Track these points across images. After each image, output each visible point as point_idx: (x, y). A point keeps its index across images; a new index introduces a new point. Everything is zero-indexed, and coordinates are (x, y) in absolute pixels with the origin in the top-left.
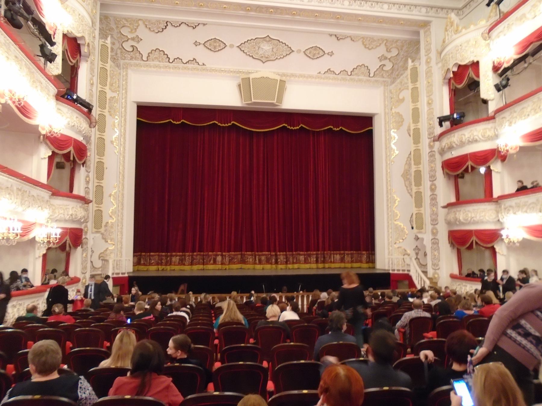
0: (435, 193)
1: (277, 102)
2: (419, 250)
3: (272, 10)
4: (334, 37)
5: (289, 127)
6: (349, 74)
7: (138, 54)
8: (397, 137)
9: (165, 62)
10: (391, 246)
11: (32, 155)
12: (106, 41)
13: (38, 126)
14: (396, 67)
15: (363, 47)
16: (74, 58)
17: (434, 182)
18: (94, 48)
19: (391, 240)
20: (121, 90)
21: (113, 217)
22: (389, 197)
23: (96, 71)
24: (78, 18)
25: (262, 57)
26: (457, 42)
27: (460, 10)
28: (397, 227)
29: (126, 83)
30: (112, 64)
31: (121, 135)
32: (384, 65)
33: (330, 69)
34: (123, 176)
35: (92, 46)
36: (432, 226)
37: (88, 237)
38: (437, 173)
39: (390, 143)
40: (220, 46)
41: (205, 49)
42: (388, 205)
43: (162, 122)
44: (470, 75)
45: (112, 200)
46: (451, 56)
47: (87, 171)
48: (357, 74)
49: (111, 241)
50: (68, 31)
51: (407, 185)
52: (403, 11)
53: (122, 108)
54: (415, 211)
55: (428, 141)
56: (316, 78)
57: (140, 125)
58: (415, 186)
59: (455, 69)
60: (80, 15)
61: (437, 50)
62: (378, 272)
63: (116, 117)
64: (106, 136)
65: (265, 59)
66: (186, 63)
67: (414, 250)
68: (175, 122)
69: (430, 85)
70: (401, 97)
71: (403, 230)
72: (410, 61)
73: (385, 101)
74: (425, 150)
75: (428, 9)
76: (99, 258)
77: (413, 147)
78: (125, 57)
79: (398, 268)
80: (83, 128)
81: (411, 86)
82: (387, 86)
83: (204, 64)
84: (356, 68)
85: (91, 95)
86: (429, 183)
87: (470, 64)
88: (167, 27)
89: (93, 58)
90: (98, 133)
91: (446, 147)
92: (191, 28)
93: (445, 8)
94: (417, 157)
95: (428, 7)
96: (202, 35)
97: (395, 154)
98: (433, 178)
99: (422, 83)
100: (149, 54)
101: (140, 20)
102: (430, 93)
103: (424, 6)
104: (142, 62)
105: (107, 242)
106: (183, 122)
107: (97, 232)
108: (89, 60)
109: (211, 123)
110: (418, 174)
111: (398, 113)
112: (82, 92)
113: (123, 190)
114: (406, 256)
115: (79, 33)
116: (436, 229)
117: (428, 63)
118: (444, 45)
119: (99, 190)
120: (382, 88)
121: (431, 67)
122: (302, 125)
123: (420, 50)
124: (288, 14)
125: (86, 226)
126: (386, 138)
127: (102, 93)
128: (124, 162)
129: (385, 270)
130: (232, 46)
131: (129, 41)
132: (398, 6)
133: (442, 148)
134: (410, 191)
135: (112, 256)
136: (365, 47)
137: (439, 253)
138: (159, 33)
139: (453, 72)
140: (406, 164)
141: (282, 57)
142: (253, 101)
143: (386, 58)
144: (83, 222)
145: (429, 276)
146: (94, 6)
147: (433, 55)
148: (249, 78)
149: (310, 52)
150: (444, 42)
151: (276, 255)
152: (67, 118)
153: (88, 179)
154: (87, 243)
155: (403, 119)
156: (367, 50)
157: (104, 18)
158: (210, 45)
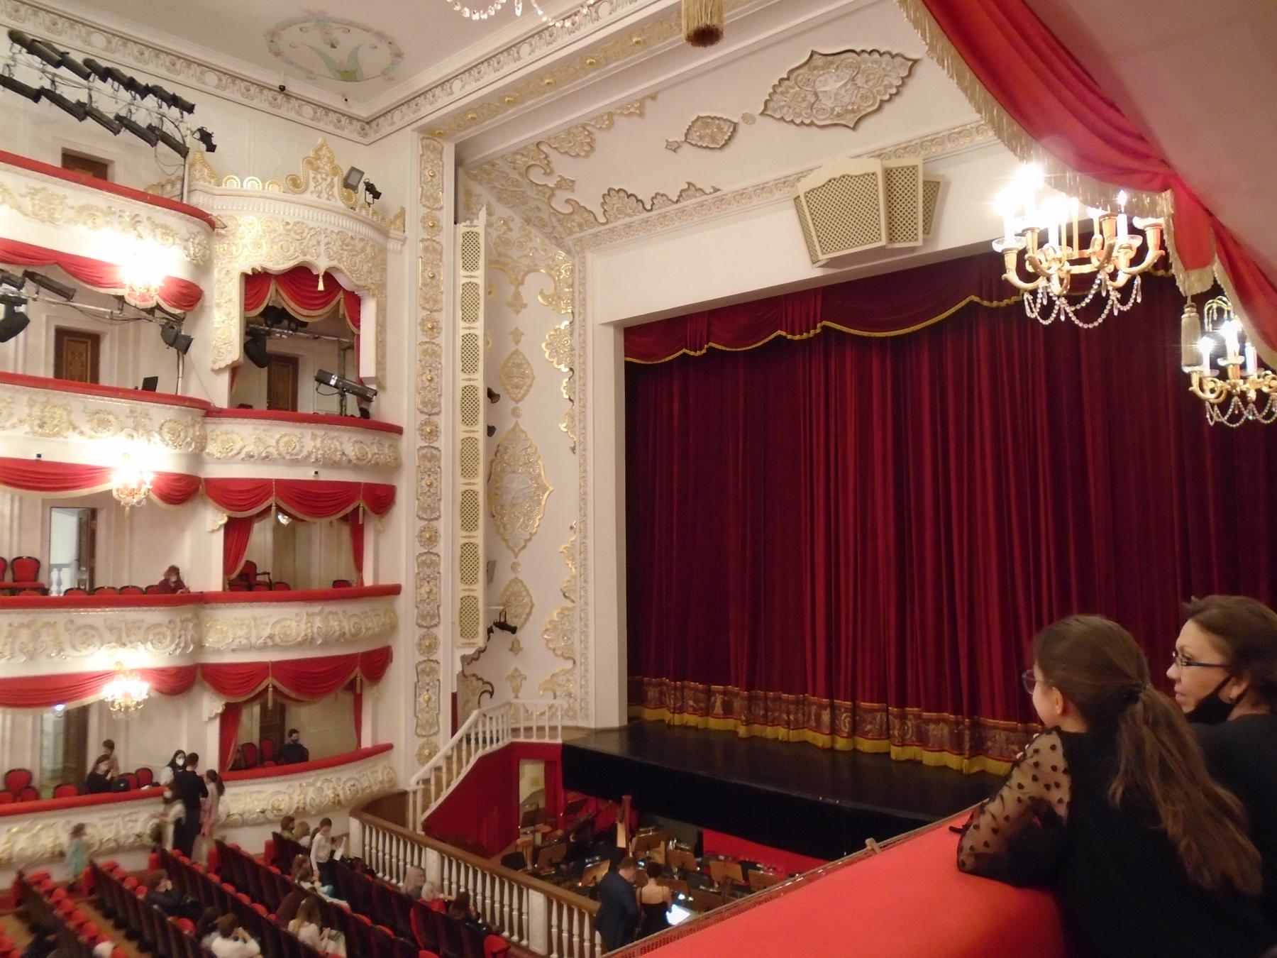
1: (891, 239)
5: (986, 303)
11: (182, 529)
13: (110, 492)
20: (577, 304)
25: (839, 115)
40: (720, 128)
43: (670, 358)
80: (305, 453)
83: (716, 190)
85: (430, 354)
101: (538, 144)
104: (602, 228)
130: (748, 119)
131: (558, 192)
141: (894, 91)
142: (824, 258)
151: (976, 726)
158: (701, 137)
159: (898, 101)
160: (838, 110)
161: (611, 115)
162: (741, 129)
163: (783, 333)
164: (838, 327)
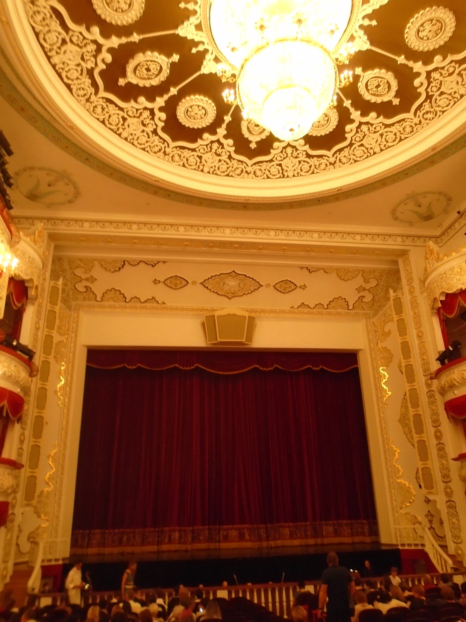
0: (441, 442)
2: (432, 516)
3: (237, 245)
4: (305, 270)
5: (262, 368)
6: (326, 307)
7: (91, 295)
8: (387, 376)
9: (122, 302)
10: (397, 512)
12: (58, 283)
14: (377, 298)
15: (338, 278)
16: (19, 301)
17: (439, 428)
18: (43, 290)
19: (395, 503)
21: (50, 484)
22: (387, 447)
23: (43, 314)
24: (27, 260)
25: (228, 293)
26: (441, 270)
27: (438, 238)
28: (401, 487)
29: (77, 325)
30: (63, 305)
31: (67, 384)
32: (364, 297)
33: (303, 303)
34: (66, 433)
35: (42, 288)
36: (445, 484)
37: (16, 511)
38: (440, 417)
39: (380, 383)
40: (181, 283)
41: (166, 287)
42: (386, 459)
44: (461, 305)
45: (50, 463)
46: (435, 285)
47: (22, 428)
48: (334, 307)
49: (45, 515)
50: (15, 274)
51: (407, 433)
52: (377, 242)
53: (70, 353)
54: (420, 465)
55: (423, 379)
56: (288, 313)
57: (90, 372)
58: (416, 433)
59: (443, 298)
60: (30, 257)
61: (420, 279)
62: (384, 548)
63: (63, 363)
64: (48, 386)
65: (230, 295)
66: (144, 302)
67: (426, 516)
68: (130, 367)
69: (417, 316)
70: (386, 330)
71: (408, 490)
72: (391, 291)
73: (368, 335)
74: (423, 391)
75: (404, 238)
76: (29, 538)
77: (407, 387)
78: (77, 298)
79: (409, 542)
80: (22, 378)
81: (396, 318)
82: (369, 319)
83: (164, 303)
84: (333, 301)
85: (35, 340)
86: (432, 431)
87: (458, 292)
88: (125, 266)
89: (41, 301)
90: (39, 382)
91: (447, 385)
92: (151, 266)
93: (422, 237)
94: (412, 398)
95: (403, 236)
96: (162, 273)
97: (387, 396)
98: (436, 423)
99: (408, 313)
100: (103, 294)
101: (96, 260)
102: (418, 324)
103: (399, 236)
104: (96, 303)
105: (39, 517)
106: (139, 367)
107: (28, 505)
108: (36, 303)
109: (172, 366)
110: (418, 419)
111: (386, 348)
112: (25, 338)
113: (64, 450)
114: (417, 526)
115: (27, 275)
116: (451, 488)
117: (411, 292)
118: (426, 274)
119: (36, 451)
120: (364, 321)
121: (416, 296)
122: (276, 365)
123: (401, 279)
124: (254, 249)
125: (15, 498)
126: (374, 376)
127: (49, 338)
128: (68, 415)
129: (392, 545)
130: (194, 283)
131: (83, 281)
132: (371, 236)
133: (442, 387)
134: (411, 440)
135: (45, 536)
136: (341, 279)
137: (459, 521)
138: (116, 273)
139: (441, 301)
140: (402, 406)
141: (250, 292)
143: (364, 289)
144: (11, 493)
145: (450, 553)
146: (47, 248)
147: (416, 283)
148: (214, 316)
149: (280, 286)
150: (426, 270)
152: (4, 367)
153: (22, 438)
154: (12, 521)
155: (392, 354)
156: (343, 282)
157: (57, 260)
158: (171, 282)
159: (249, 295)
160: (229, 291)
161: (140, 262)
162: (188, 285)
163: (178, 366)
164: (203, 367)
